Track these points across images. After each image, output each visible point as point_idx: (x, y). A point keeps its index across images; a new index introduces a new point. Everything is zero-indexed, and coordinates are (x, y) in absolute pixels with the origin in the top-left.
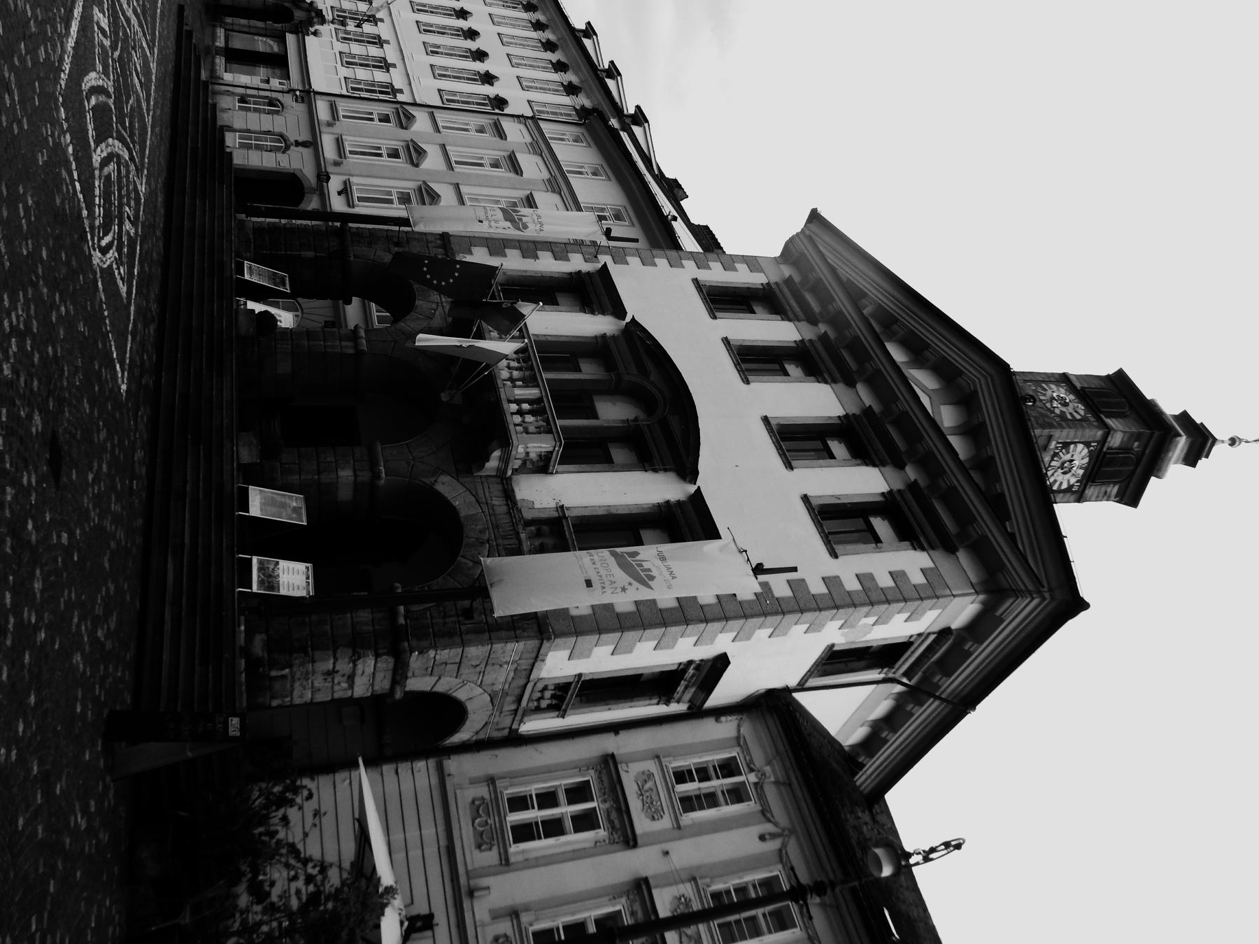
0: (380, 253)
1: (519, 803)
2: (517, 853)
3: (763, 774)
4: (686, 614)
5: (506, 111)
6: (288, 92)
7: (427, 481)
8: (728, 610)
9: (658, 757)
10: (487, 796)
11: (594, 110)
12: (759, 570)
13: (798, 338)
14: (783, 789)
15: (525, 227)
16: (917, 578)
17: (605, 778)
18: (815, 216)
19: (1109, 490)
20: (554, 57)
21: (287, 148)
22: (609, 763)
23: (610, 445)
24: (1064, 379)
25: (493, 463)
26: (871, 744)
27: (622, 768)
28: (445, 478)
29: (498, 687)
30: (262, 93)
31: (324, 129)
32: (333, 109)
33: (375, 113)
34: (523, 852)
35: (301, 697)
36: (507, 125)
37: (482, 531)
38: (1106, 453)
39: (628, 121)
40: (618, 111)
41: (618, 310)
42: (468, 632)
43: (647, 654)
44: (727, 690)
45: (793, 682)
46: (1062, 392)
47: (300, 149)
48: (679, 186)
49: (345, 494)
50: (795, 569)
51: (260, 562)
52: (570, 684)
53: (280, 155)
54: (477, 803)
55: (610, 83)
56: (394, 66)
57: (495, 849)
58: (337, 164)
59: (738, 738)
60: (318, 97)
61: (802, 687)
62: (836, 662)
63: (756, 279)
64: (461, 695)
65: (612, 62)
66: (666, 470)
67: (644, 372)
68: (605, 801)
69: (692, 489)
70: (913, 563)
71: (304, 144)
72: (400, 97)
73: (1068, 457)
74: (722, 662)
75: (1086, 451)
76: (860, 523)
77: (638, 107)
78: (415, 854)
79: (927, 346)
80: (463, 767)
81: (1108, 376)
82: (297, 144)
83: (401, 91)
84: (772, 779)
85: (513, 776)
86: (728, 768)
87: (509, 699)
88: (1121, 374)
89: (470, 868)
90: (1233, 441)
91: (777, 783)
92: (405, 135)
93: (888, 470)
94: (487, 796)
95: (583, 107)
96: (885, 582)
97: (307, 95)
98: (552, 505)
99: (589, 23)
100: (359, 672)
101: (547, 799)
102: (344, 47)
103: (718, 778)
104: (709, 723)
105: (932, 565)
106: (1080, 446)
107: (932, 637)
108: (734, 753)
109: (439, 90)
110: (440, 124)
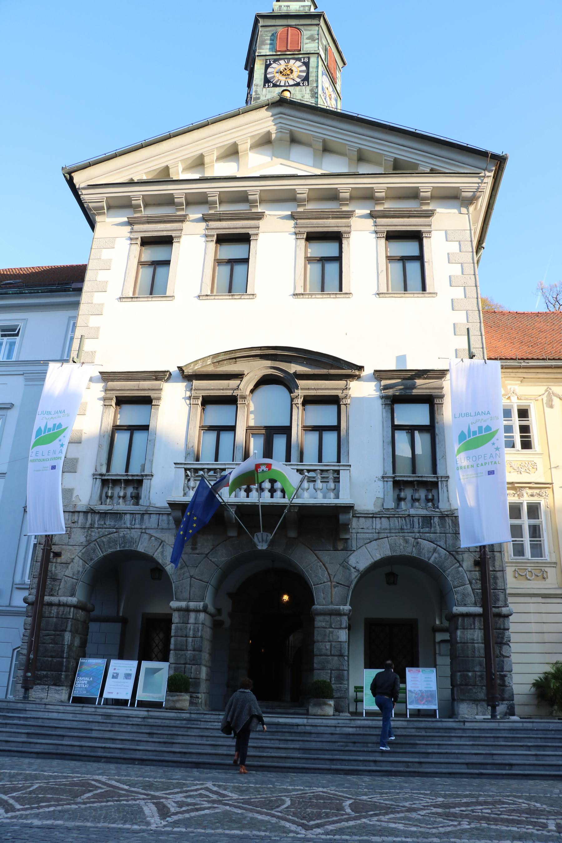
0: (69, 572)
2: (550, 557)
7: (354, 576)
10: (513, 568)
28: (352, 560)
34: (550, 553)
37: (406, 542)
42: (494, 566)
50: (468, 329)
51: (410, 704)
54: (517, 575)
57: (546, 569)
78: (545, 618)
89: (557, 586)
98: (381, 484)
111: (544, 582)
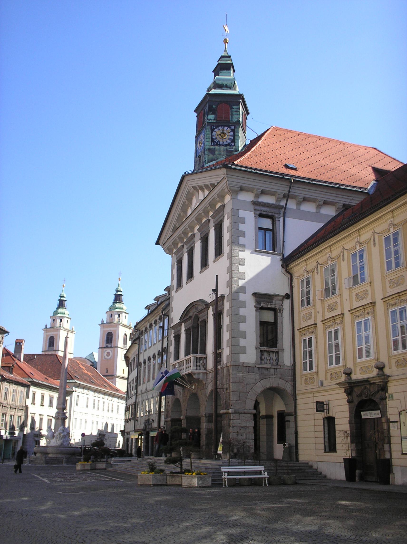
18: (157, 243)
19: (235, 110)
24: (197, 137)
25: (201, 377)
29: (258, 377)
38: (217, 120)
45: (279, 258)
50: (217, 276)
65: (154, 300)
66: (208, 314)
67: (191, 317)
87: (266, 372)
90: (225, 42)
100: (239, 425)
106: (214, 133)
107: (257, 208)
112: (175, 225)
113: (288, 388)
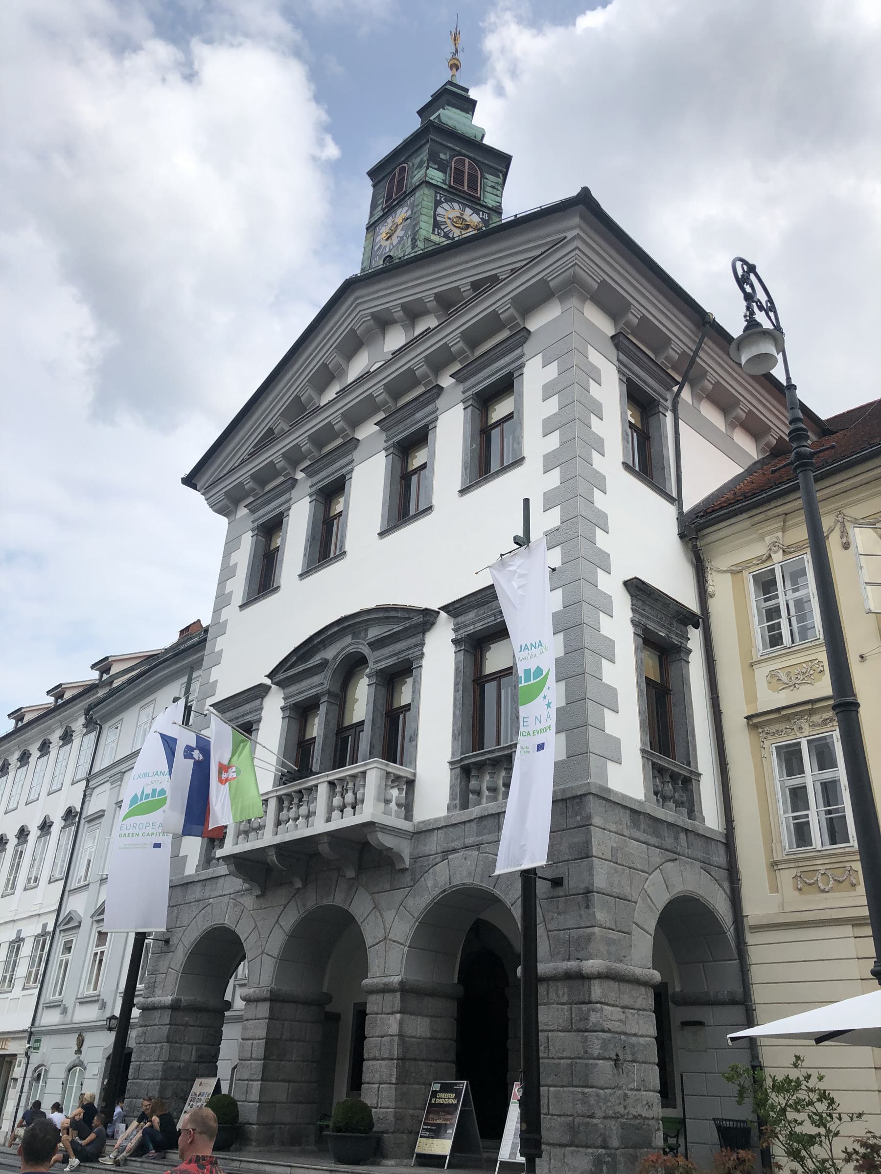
1: (802, 833)
3: (774, 544)
4: (572, 624)
5: (78, 810)
6: (28, 1058)
8: (574, 578)
9: (751, 665)
10: (793, 872)
11: (86, 714)
12: (523, 541)
13: (308, 499)
14: (788, 523)
15: (163, 792)
16: (552, 371)
17: (773, 728)
18: (190, 481)
19: (490, 184)
20: (35, 753)
21: (81, 1064)
22: (756, 722)
23: (396, 706)
24: (372, 227)
26: (754, 428)
27: (762, 706)
30: (26, 1089)
31: (68, 1019)
32: (51, 1006)
33: (61, 957)
35: (650, 1106)
36: (92, 808)
38: (450, 186)
39: (105, 676)
40: (91, 688)
41: (258, 692)
43: (622, 672)
44: (675, 582)
45: (671, 511)
46: (383, 230)
47: (84, 1049)
48: (188, 628)
49: (420, 1027)
50: (527, 501)
52: (654, 764)
53: (88, 1074)
55: (68, 695)
56: (19, 932)
58: (103, 1006)
59: (733, 573)
60: (37, 1023)
61: (677, 501)
62: (649, 463)
63: (247, 541)
64: (662, 899)
65: (48, 693)
66: (423, 644)
67: (325, 664)
68: (800, 728)
69: (443, 614)
70: (536, 374)
71: (80, 1043)
72: (50, 928)
73: (448, 221)
74: (637, 588)
75: (445, 205)
76: (495, 433)
77: (93, 667)
79: (325, 366)
80: (758, 903)
81: (374, 186)
82: (79, 1051)
83: (45, 926)
84: (780, 534)
85: (769, 839)
86: (766, 585)
88: (372, 174)
91: (784, 530)
92: (87, 922)
93: (441, 403)
94: (793, 872)
95: (86, 726)
96: (553, 406)
97: (32, 1035)
99: (9, 716)
101: (798, 797)
102: (19, 984)
103: (777, 597)
104: (713, 605)
105: (540, 357)
106: (440, 210)
108: (748, 578)
109: (50, 882)
110: (82, 883)
111: (853, 893)
112: (271, 431)
113: (721, 905)
